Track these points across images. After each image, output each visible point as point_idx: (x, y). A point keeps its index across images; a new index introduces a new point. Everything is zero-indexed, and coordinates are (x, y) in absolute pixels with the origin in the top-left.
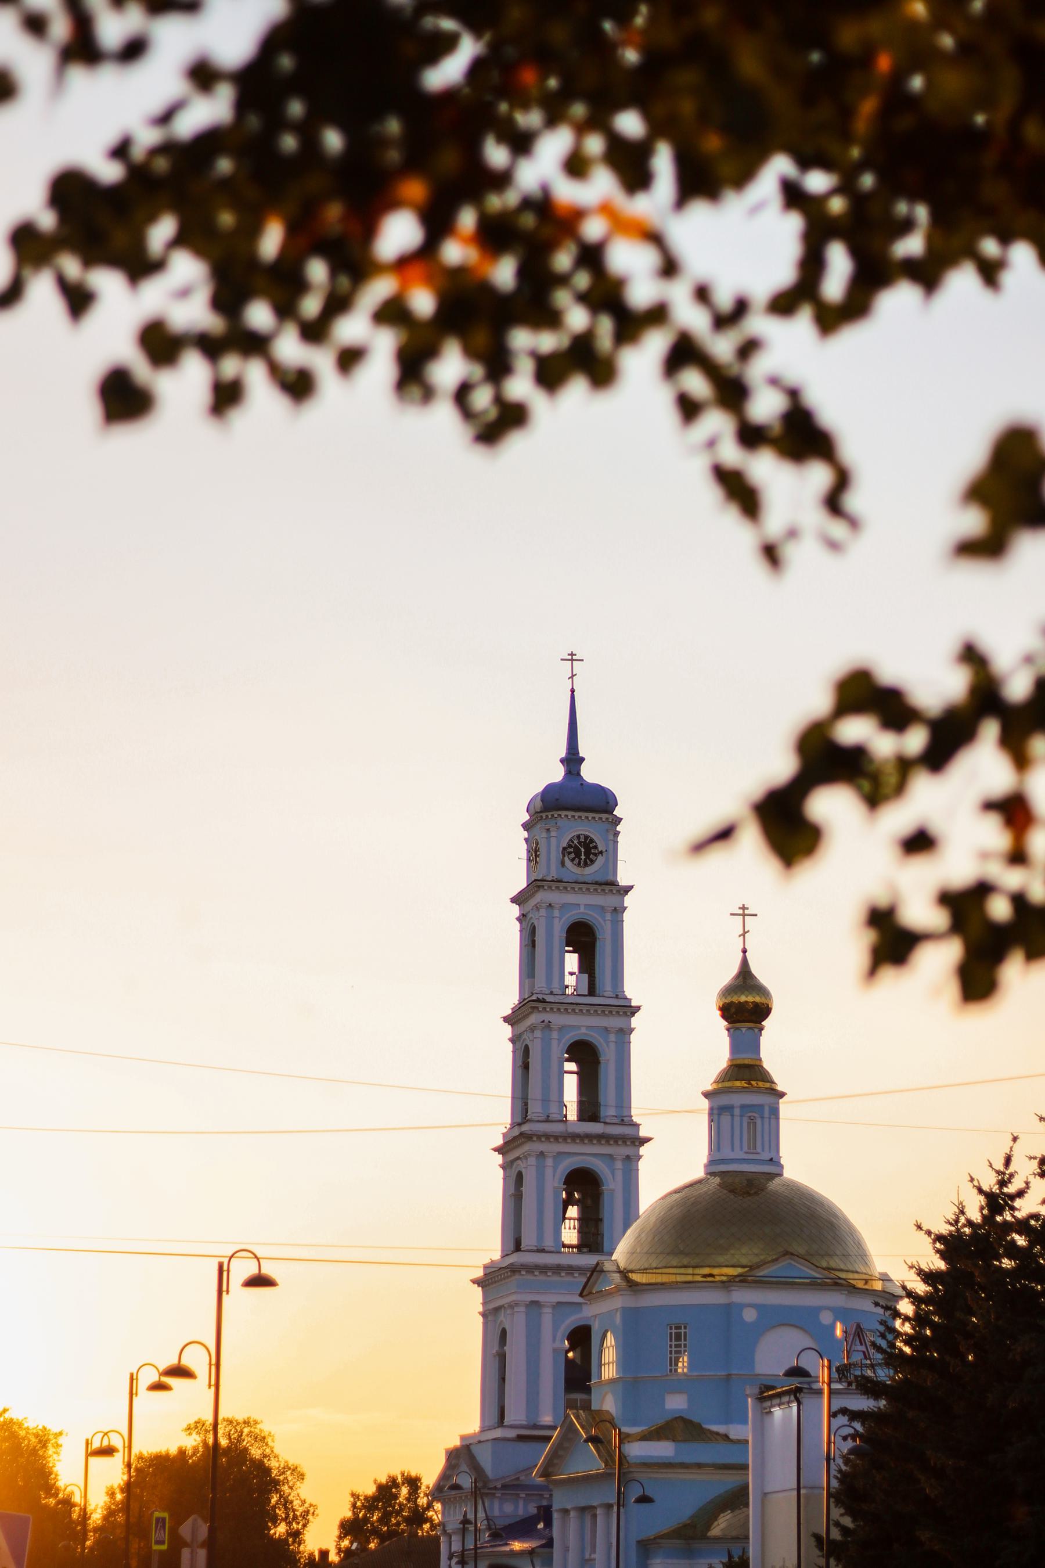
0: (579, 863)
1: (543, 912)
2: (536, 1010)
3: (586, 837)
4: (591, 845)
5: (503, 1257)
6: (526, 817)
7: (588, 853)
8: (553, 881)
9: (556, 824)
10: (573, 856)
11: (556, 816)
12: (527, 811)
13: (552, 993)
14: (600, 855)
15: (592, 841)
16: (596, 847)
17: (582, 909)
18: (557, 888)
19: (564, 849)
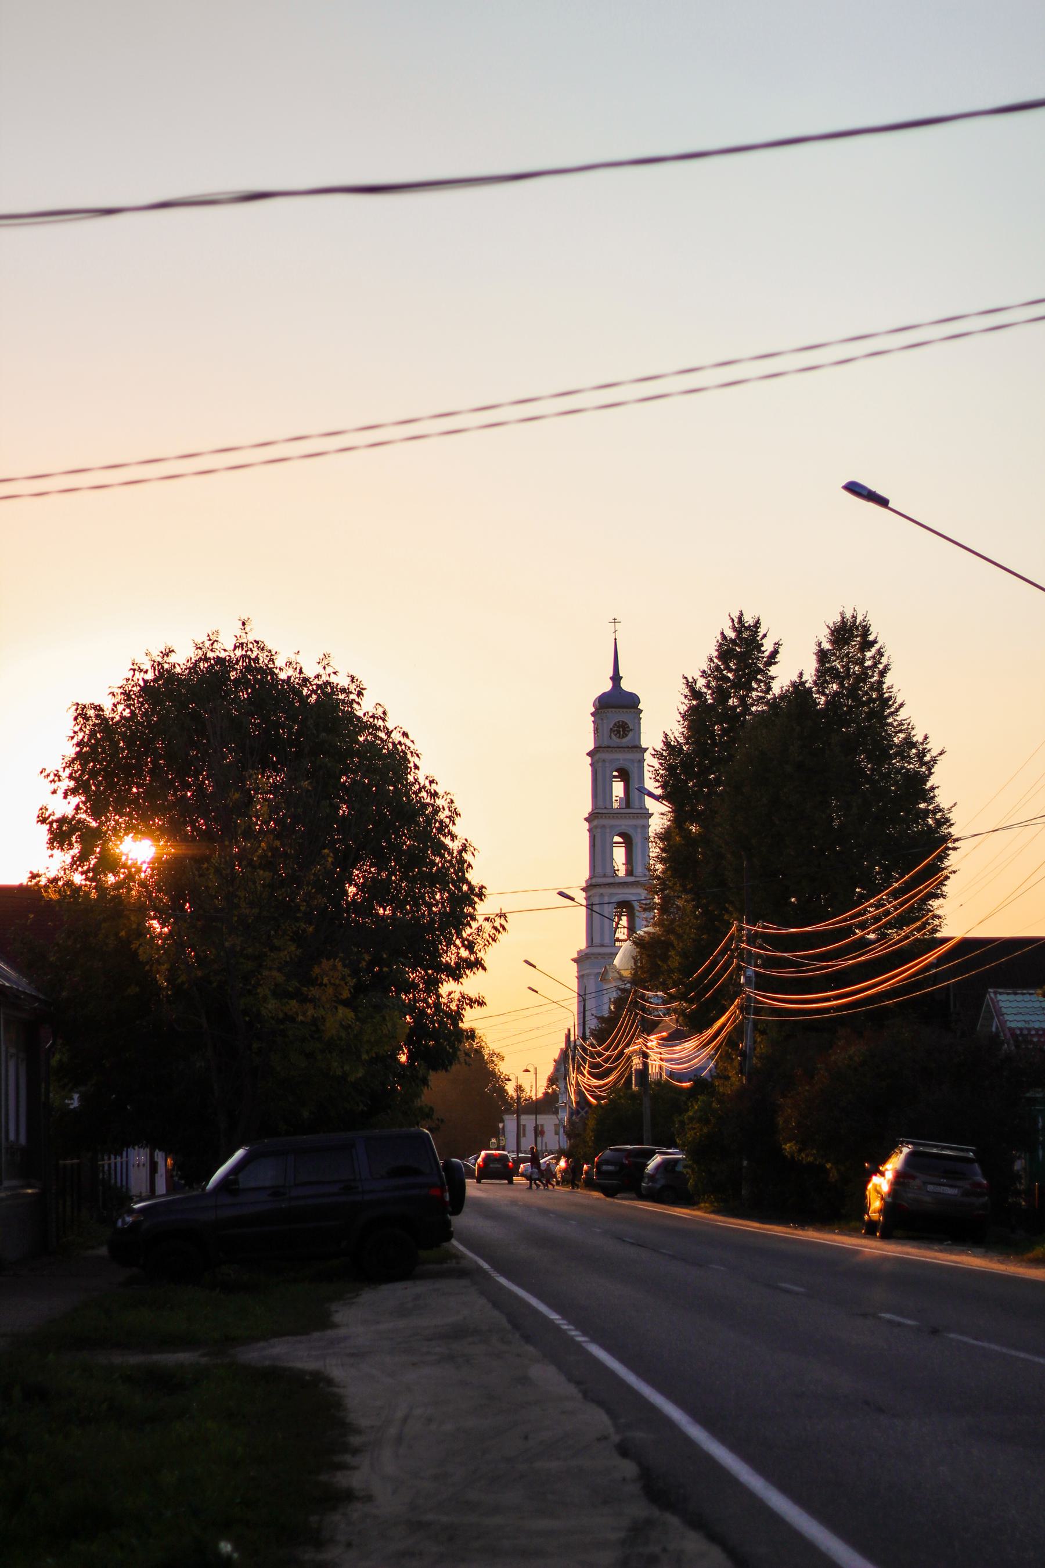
0: (619, 736)
1: (600, 764)
3: (623, 722)
4: (626, 726)
5: (586, 948)
6: (593, 710)
7: (624, 731)
8: (605, 747)
10: (616, 732)
12: (593, 706)
13: (605, 808)
15: (626, 724)
16: (628, 727)
17: (621, 762)
18: (607, 751)
19: (611, 729)
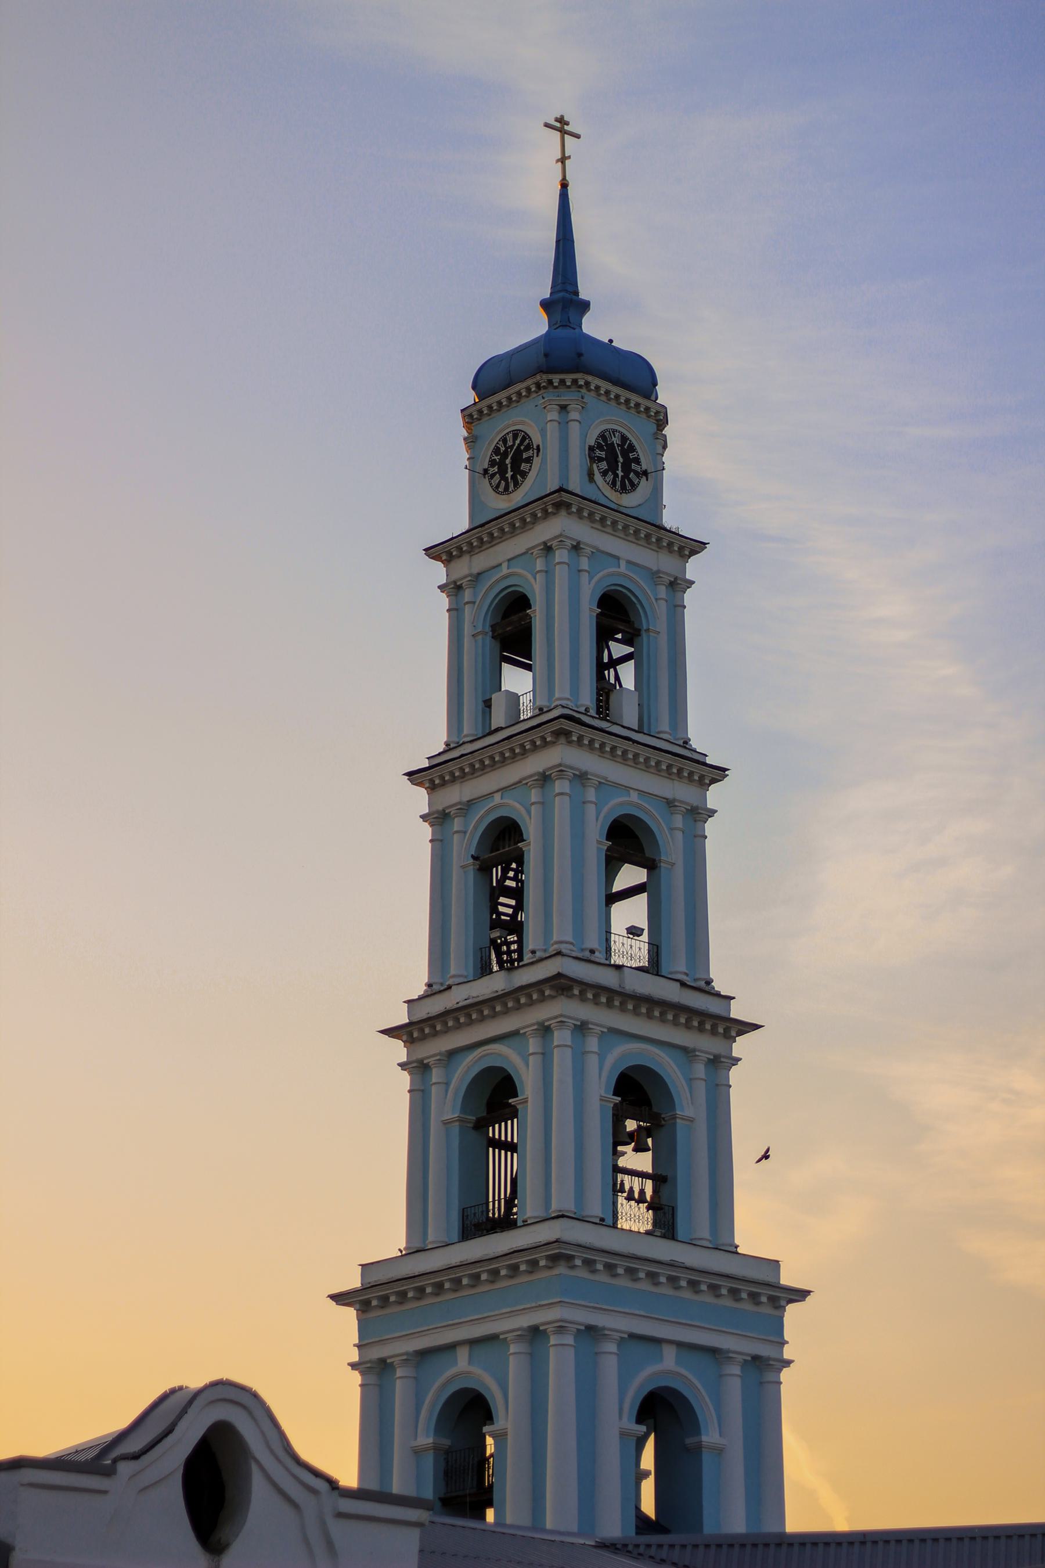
0: (614, 484)
2: (562, 740)
7: (627, 469)
9: (582, 398)
10: (604, 465)
11: (581, 382)
14: (644, 478)
15: (632, 448)
16: (637, 461)
17: (623, 568)
19: (591, 449)
